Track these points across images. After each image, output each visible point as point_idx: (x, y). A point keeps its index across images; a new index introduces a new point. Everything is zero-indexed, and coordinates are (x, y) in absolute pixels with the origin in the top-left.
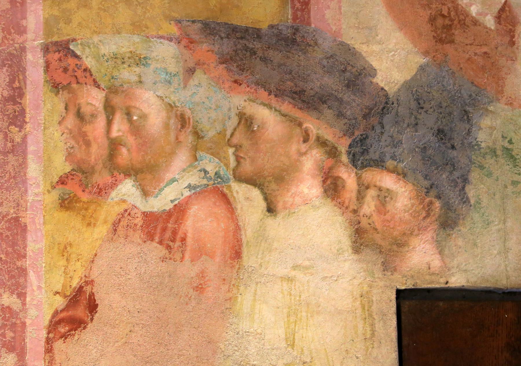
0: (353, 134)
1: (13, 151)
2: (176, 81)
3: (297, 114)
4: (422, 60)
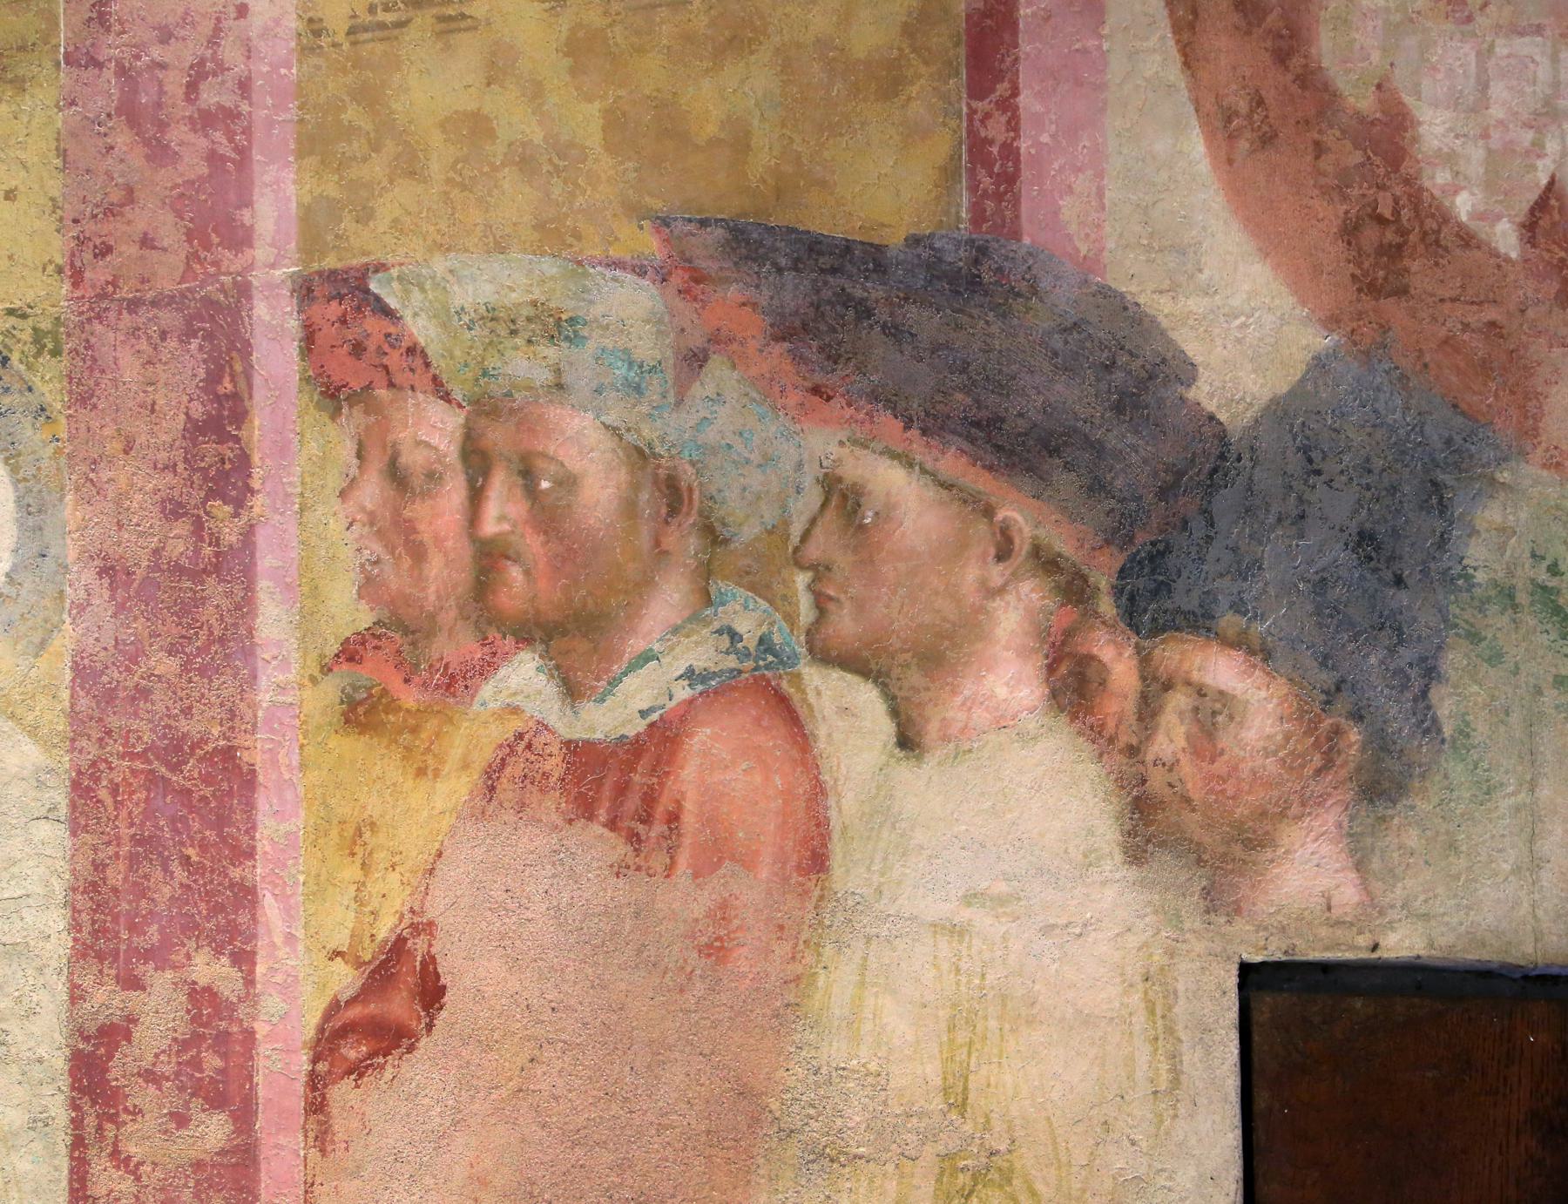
0: (1131, 539)
1: (217, 568)
2: (654, 387)
3: (980, 481)
4: (1321, 341)
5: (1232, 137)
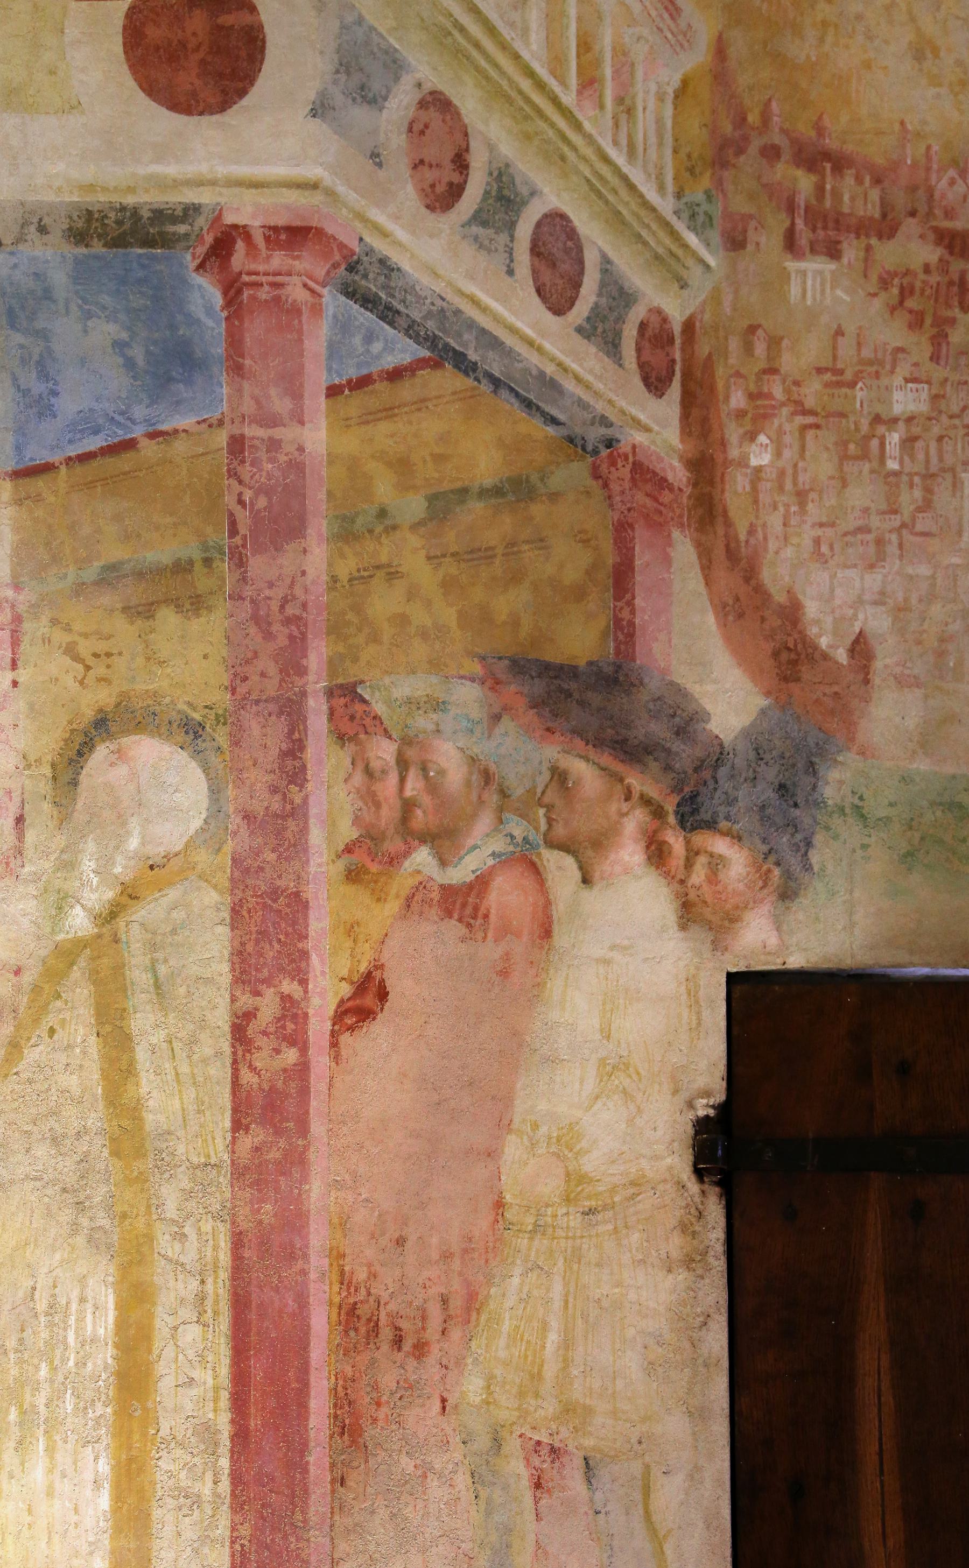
0: (682, 790)
4: (763, 702)
5: (726, 615)
